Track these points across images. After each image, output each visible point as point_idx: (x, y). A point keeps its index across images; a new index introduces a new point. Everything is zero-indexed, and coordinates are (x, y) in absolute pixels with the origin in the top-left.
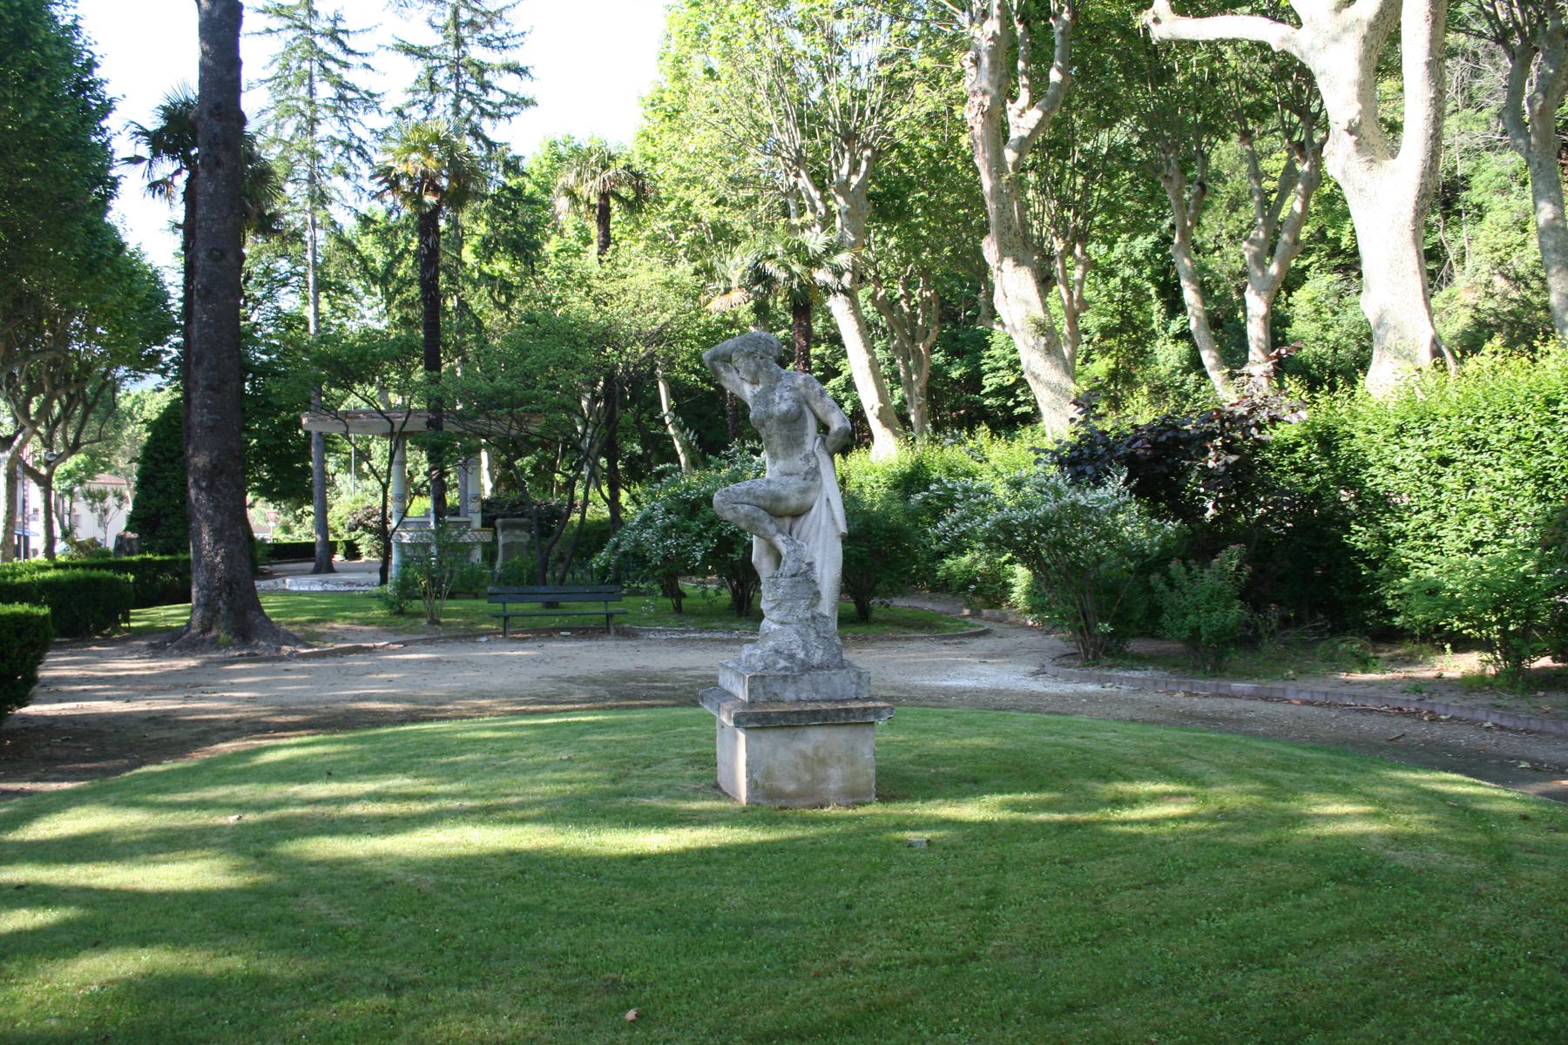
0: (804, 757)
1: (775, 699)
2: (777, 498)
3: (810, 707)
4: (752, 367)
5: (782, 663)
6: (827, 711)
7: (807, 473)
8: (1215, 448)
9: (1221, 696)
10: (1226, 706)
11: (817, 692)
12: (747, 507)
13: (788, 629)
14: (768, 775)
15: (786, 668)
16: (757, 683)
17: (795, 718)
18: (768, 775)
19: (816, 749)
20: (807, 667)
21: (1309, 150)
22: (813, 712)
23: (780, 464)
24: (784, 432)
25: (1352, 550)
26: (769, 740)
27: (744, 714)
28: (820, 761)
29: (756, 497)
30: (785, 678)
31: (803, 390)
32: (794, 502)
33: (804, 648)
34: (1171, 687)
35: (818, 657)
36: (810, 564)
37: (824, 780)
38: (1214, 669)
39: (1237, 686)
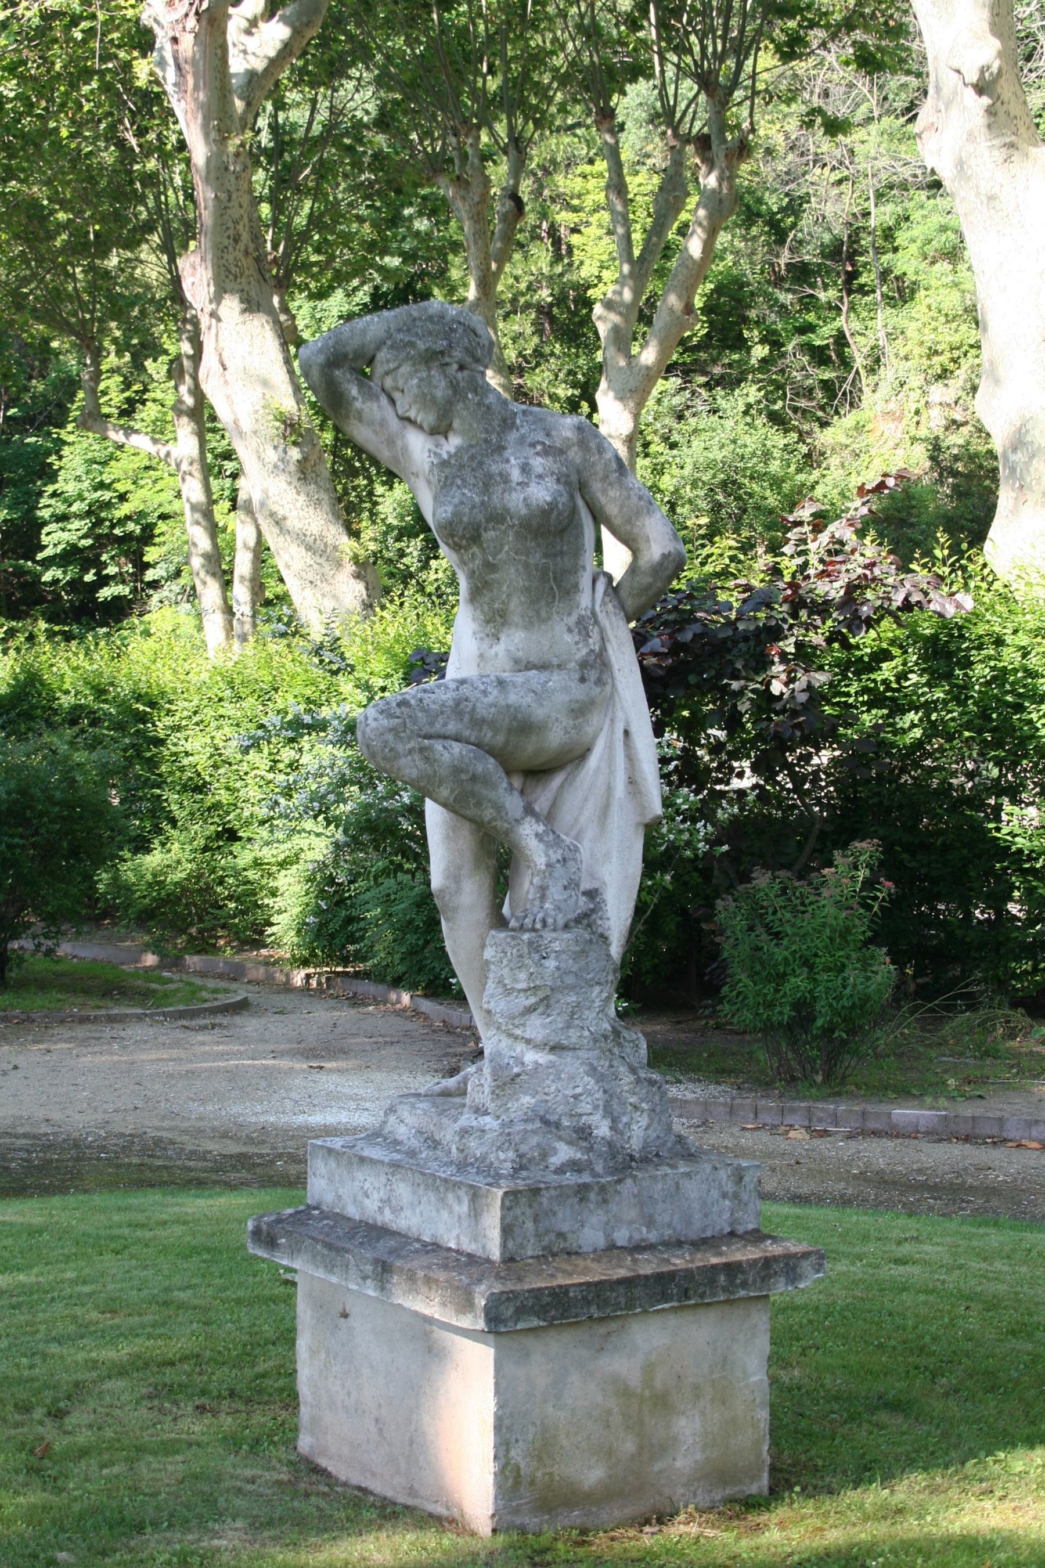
0: (625, 1392)
1: (559, 1250)
2: (524, 726)
3: (648, 1266)
4: (441, 390)
5: (564, 1153)
6: (689, 1274)
7: (584, 665)
8: (784, 656)
9: (876, 1133)
10: (879, 1154)
11: (650, 1223)
12: (457, 748)
13: (570, 1064)
14: (545, 1448)
15: (574, 1166)
16: (521, 1209)
17: (620, 1296)
18: (545, 1448)
19: (649, 1369)
20: (625, 1163)
21: (717, 150)
22: (660, 1278)
23: (515, 640)
24: (536, 558)
25: (1003, 851)
26: (553, 1353)
27: (508, 1297)
28: (651, 1403)
29: (477, 723)
30: (582, 1190)
31: (575, 454)
32: (555, 738)
33: (608, 1111)
34: (765, 1118)
35: (638, 1132)
36: (592, 894)
37: (664, 1448)
38: (828, 1077)
39: (904, 1113)
